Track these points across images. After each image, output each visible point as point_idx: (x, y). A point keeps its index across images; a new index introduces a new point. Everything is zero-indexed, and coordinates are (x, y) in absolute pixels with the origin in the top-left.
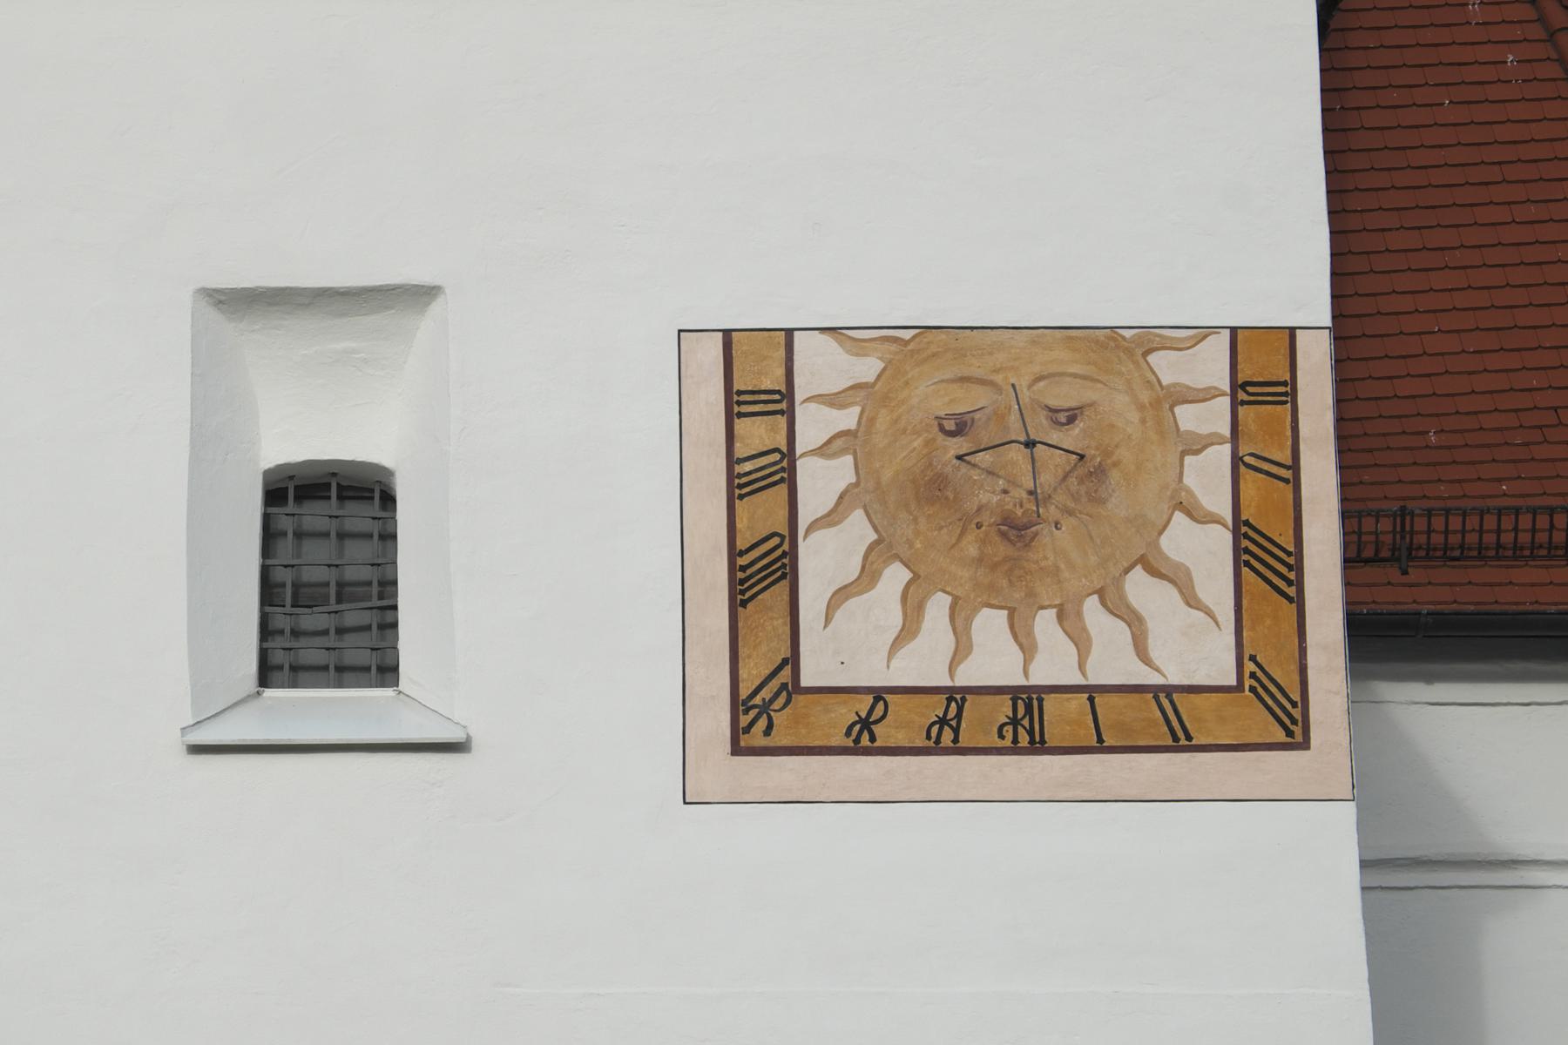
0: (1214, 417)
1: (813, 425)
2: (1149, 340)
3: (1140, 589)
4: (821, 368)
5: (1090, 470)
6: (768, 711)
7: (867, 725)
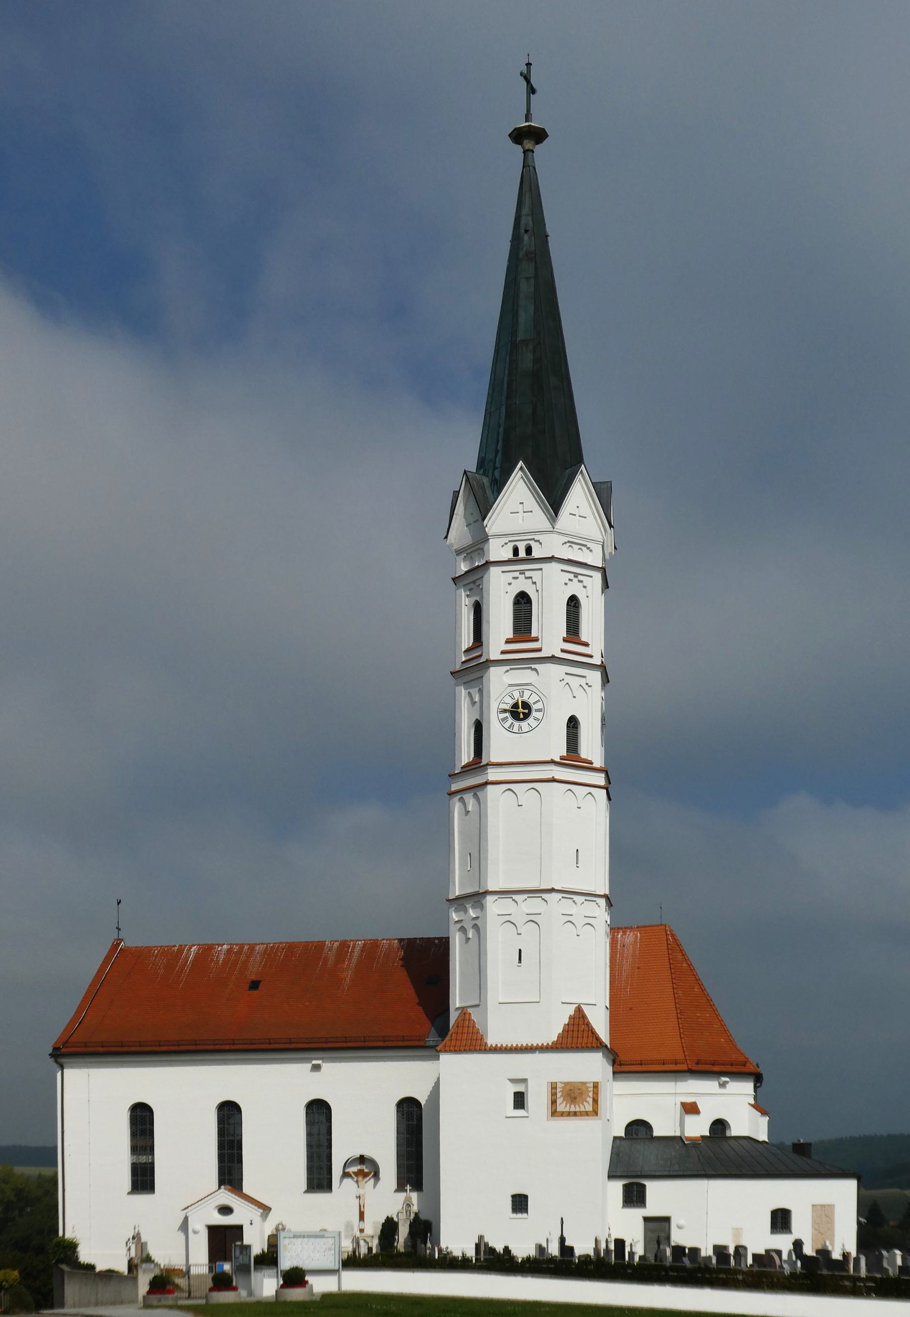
1: (558, 1090)
4: (559, 1085)
5: (581, 1094)
6: (554, 1113)
7: (562, 1114)
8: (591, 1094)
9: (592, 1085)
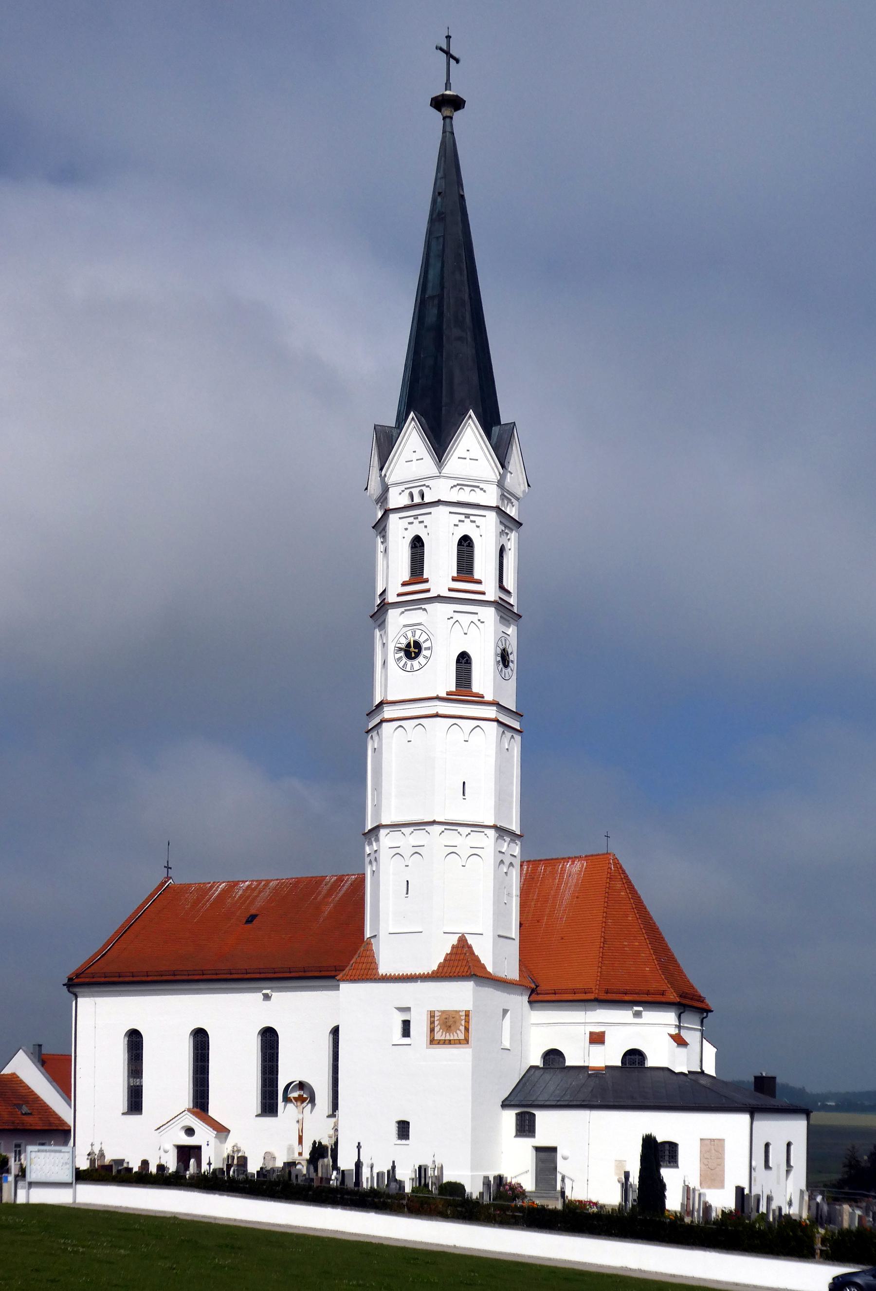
0: (463, 1017)
5: (455, 1022)
6: (432, 1041)
7: (439, 1042)
8: (463, 1022)
9: (463, 1013)
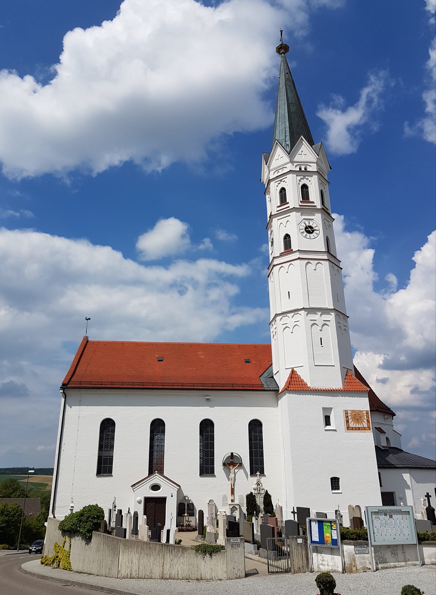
0: (365, 415)
1: (349, 415)
2: (363, 411)
3: (363, 423)
4: (349, 412)
6: (348, 428)
8: (365, 417)
